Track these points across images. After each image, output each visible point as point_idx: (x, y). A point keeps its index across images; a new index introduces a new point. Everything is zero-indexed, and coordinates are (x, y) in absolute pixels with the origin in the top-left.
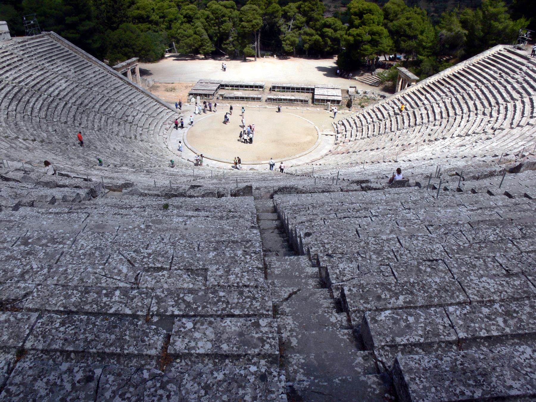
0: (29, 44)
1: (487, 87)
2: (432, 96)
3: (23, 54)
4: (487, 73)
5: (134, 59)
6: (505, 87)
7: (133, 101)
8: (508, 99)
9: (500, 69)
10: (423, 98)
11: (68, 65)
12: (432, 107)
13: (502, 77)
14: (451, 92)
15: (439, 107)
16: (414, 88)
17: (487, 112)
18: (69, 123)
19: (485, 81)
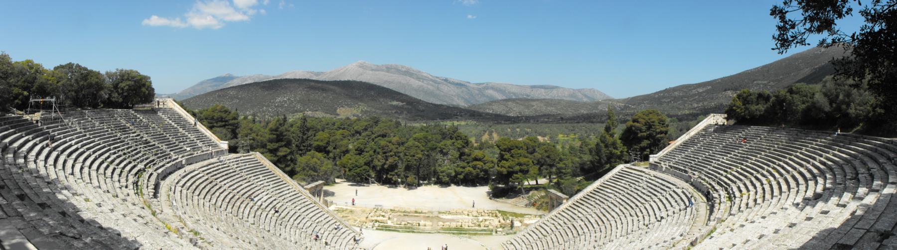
0: (241, 160)
1: (624, 196)
2: (583, 209)
3: (236, 168)
4: (619, 185)
5: (320, 182)
6: (637, 194)
7: (320, 219)
8: (643, 201)
9: (628, 182)
10: (576, 212)
11: (269, 180)
12: (587, 218)
13: (631, 186)
14: (597, 203)
15: (592, 217)
16: (566, 204)
17: (633, 213)
18: (271, 232)
19: (620, 191)
